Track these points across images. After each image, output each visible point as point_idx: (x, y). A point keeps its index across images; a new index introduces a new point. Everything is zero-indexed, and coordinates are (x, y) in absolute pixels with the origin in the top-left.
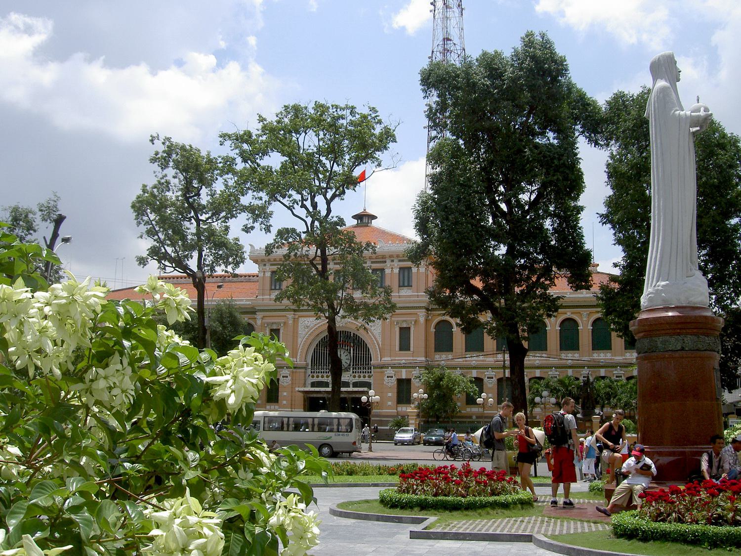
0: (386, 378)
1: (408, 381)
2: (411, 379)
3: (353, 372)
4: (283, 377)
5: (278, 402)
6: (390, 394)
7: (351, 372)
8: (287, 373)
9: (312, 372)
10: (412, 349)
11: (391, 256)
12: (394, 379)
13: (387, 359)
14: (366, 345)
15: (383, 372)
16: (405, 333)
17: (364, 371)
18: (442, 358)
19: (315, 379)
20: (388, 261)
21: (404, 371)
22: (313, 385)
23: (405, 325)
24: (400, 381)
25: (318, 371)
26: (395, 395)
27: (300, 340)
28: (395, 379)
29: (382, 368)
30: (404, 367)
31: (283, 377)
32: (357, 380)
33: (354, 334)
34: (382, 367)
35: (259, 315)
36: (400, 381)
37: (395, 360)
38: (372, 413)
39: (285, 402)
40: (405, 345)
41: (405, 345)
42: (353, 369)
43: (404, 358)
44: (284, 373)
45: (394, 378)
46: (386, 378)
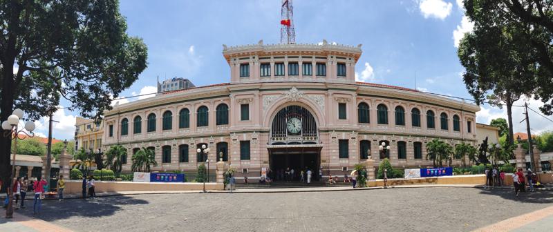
1: (346, 141)
2: (348, 140)
5: (250, 159)
10: (348, 117)
11: (333, 53)
13: (331, 125)
16: (342, 107)
19: (275, 141)
20: (329, 56)
22: (273, 144)
23: (342, 102)
24: (340, 141)
26: (338, 151)
29: (328, 131)
30: (344, 131)
32: (306, 141)
35: (232, 95)
36: (340, 141)
39: (255, 159)
40: (342, 115)
41: (342, 115)
43: (343, 124)
45: (337, 139)
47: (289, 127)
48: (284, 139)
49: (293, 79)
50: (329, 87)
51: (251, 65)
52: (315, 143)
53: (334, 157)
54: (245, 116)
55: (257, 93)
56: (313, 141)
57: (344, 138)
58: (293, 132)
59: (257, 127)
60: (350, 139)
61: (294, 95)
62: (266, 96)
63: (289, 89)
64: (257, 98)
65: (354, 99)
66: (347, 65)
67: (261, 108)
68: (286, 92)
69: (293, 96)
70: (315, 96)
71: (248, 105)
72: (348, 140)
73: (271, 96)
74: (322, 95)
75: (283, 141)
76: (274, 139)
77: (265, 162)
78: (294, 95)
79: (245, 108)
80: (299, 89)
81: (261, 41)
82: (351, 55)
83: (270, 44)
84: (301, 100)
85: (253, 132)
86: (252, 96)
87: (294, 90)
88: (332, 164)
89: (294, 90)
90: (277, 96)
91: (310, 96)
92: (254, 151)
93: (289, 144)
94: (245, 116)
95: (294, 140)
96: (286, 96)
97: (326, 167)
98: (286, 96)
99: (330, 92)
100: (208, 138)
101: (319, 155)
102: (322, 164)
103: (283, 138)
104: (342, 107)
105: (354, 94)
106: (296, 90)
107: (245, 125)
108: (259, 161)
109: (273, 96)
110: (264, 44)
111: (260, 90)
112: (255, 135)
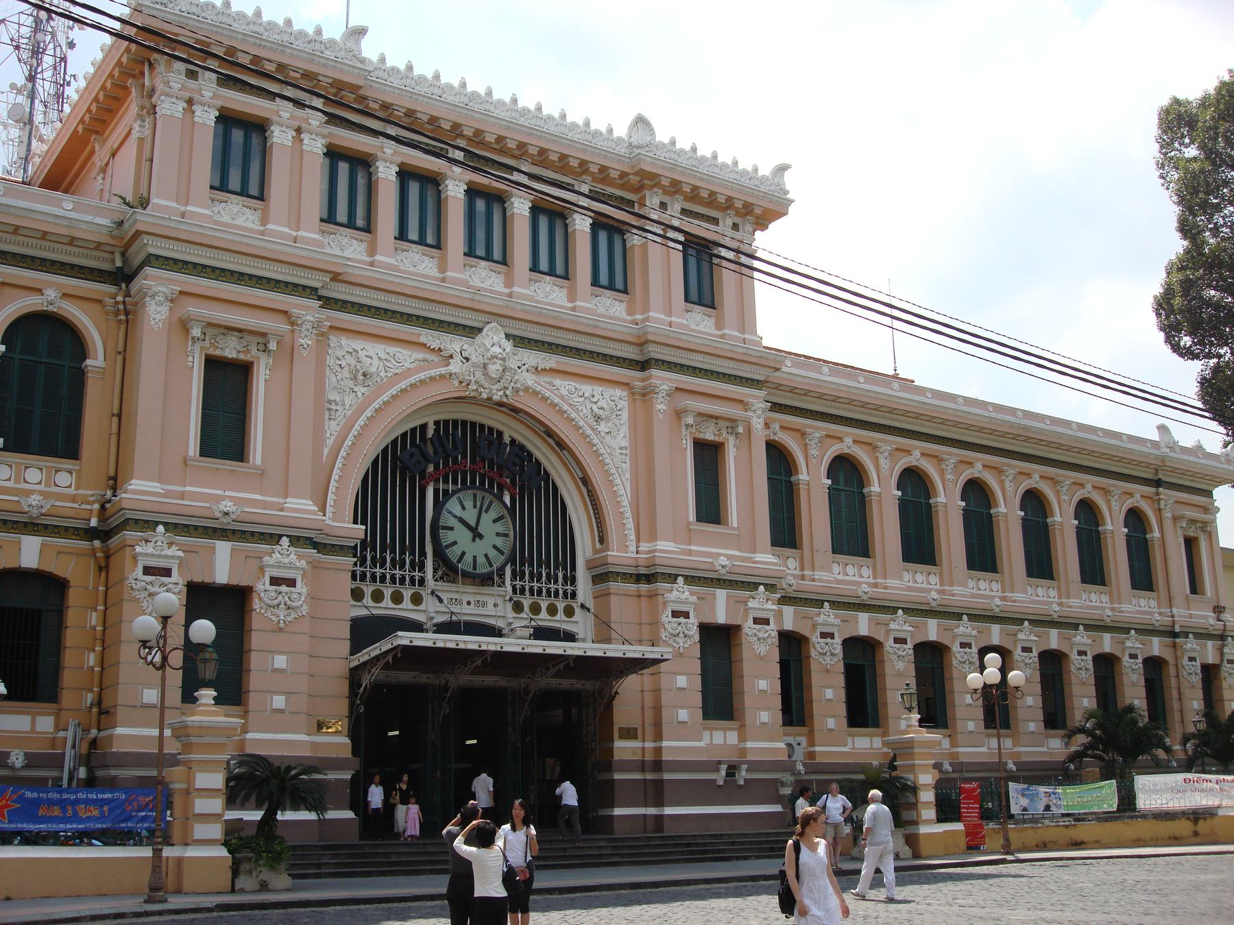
0: (666, 617)
2: (738, 628)
3: (514, 591)
4: (275, 581)
7: (509, 589)
8: (291, 567)
9: (354, 577)
11: (675, 187)
12: (691, 626)
13: (667, 549)
14: (555, 488)
15: (652, 596)
17: (552, 586)
21: (721, 594)
25: (398, 573)
27: (332, 429)
28: (697, 624)
29: (649, 578)
31: (275, 581)
33: (513, 441)
34: (648, 576)
37: (690, 553)
38: (616, 757)
39: (279, 702)
42: (514, 577)
44: (279, 565)
45: (693, 622)
46: (666, 617)
47: (447, 537)
48: (417, 599)
49: (484, 279)
50: (655, 352)
51: (280, 136)
52: (570, 637)
53: (683, 715)
54: (225, 433)
55: (307, 311)
56: (559, 622)
57: (721, 618)
58: (466, 565)
59: (299, 507)
60: (749, 627)
61: (494, 369)
62: (344, 341)
63: (472, 332)
64: (306, 340)
65: (758, 423)
67: (322, 406)
68: (454, 344)
70: (587, 389)
71: (244, 370)
72: (738, 628)
73: (357, 344)
74: (618, 392)
75: (406, 610)
76: (357, 595)
78: (494, 369)
79: (227, 386)
80: (521, 342)
81: (361, 32)
82: (747, 210)
83: (396, 61)
85: (274, 539)
86: (281, 326)
87: (494, 340)
88: (674, 746)
89: (494, 340)
90: (407, 357)
91: (564, 386)
93: (442, 628)
94: (225, 433)
95: (467, 612)
96: (455, 366)
97: (642, 766)
98: (455, 366)
99: (663, 380)
101: (606, 702)
102: (623, 748)
103: (407, 593)
104: (708, 457)
105: (757, 399)
106: (508, 345)
107: (223, 493)
108: (296, 708)
109: (380, 349)
110: (370, 49)
111: (329, 303)
112: (285, 558)
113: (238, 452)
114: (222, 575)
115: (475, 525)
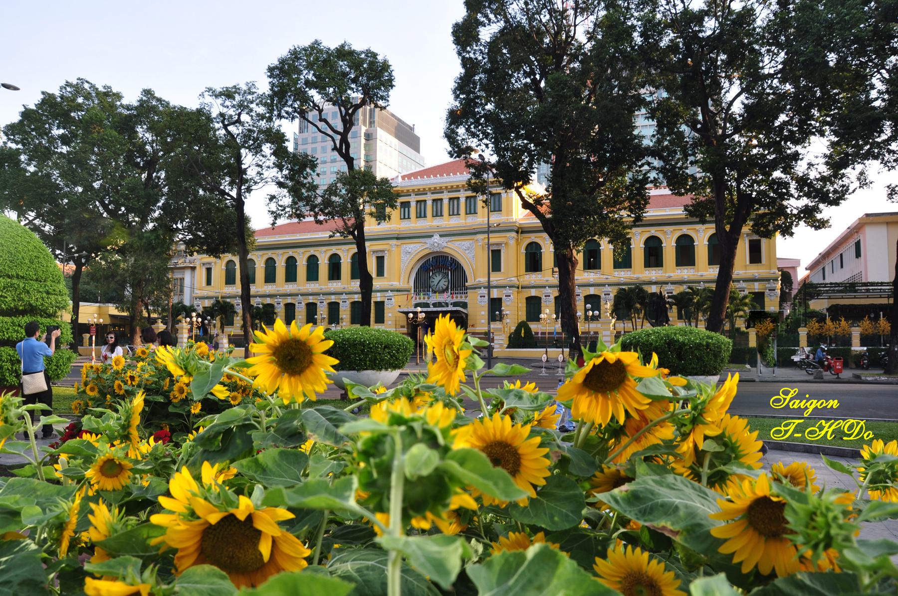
6: (483, 313)
18: (534, 278)
29: (475, 288)
32: (455, 300)
49: (437, 222)
55: (394, 242)
60: (504, 298)
66: (504, 195)
69: (438, 243)
77: (402, 327)
80: (441, 236)
84: (446, 250)
87: (436, 238)
89: (436, 238)
90: (418, 245)
91: (457, 243)
92: (388, 315)
100: (317, 297)
109: (412, 246)
112: (390, 293)
113: (383, 275)
114: (379, 300)
115: (438, 280)
